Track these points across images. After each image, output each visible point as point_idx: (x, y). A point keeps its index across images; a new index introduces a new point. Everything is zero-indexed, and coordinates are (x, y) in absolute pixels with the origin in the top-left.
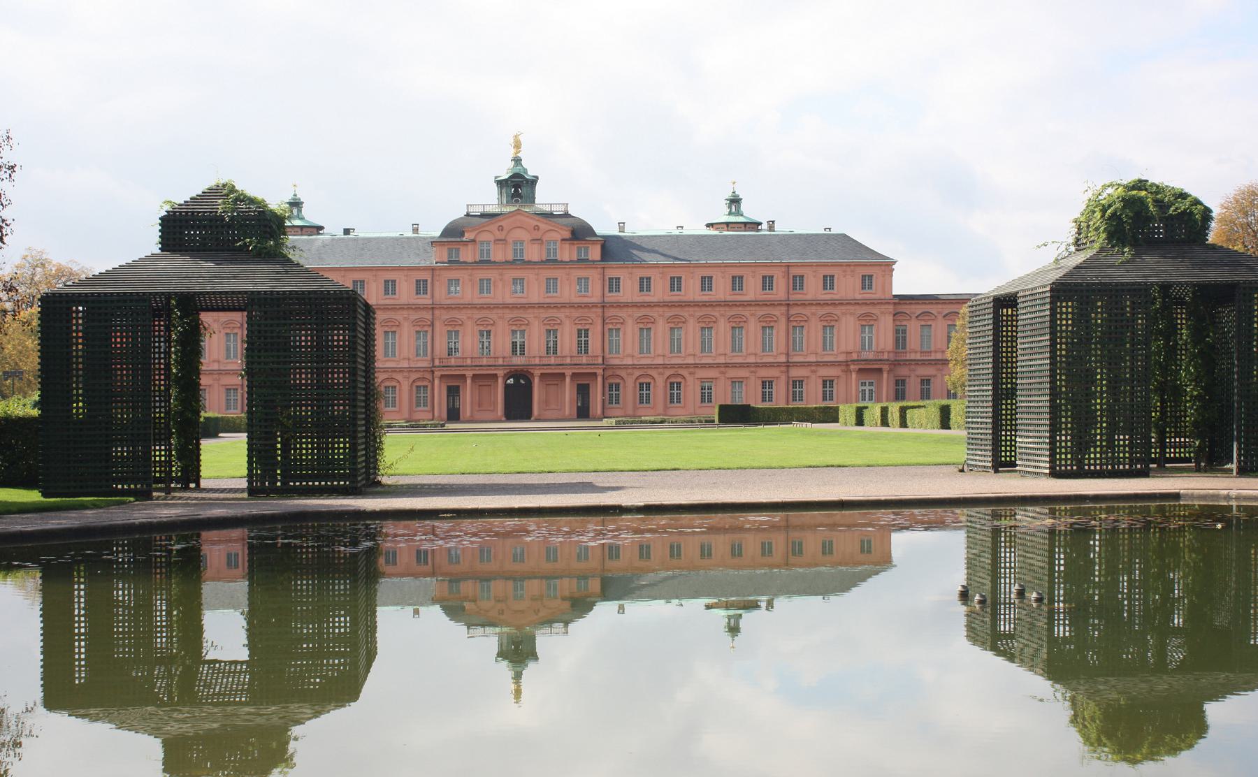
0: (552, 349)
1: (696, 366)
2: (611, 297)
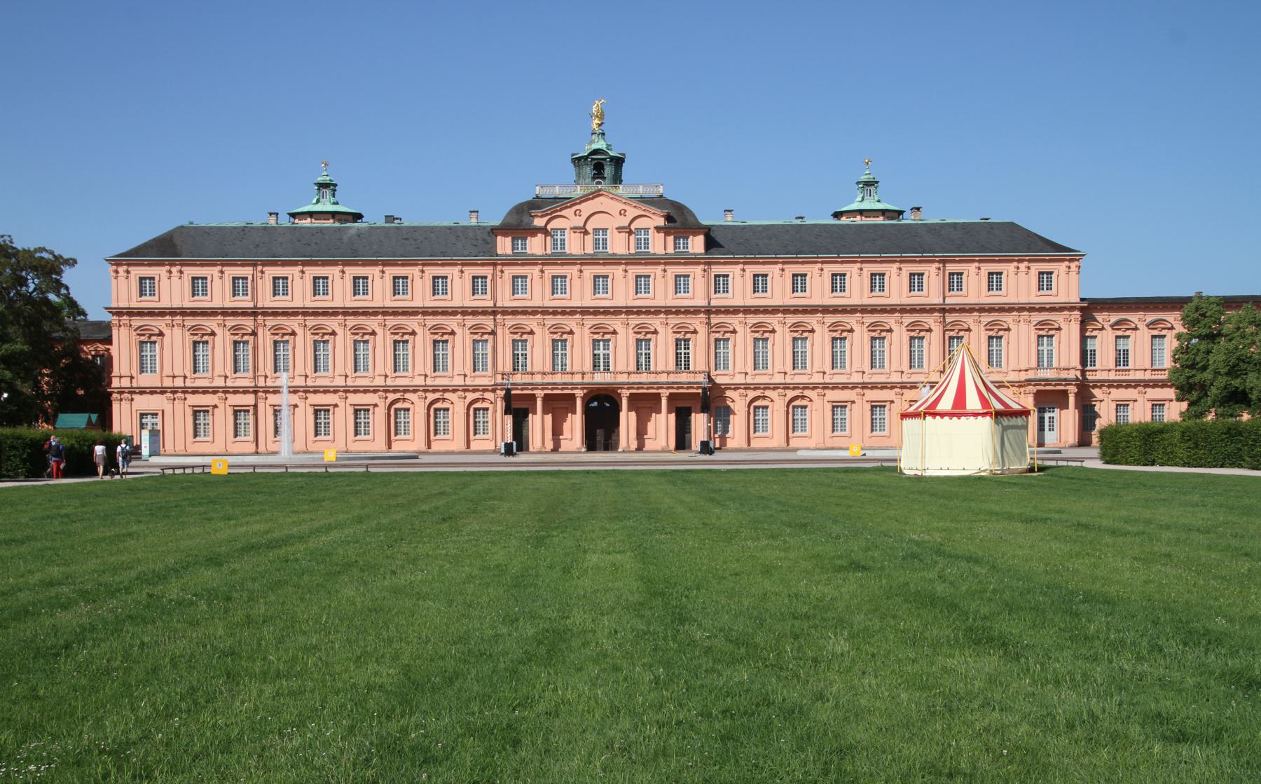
1: (826, 386)
2: (718, 301)
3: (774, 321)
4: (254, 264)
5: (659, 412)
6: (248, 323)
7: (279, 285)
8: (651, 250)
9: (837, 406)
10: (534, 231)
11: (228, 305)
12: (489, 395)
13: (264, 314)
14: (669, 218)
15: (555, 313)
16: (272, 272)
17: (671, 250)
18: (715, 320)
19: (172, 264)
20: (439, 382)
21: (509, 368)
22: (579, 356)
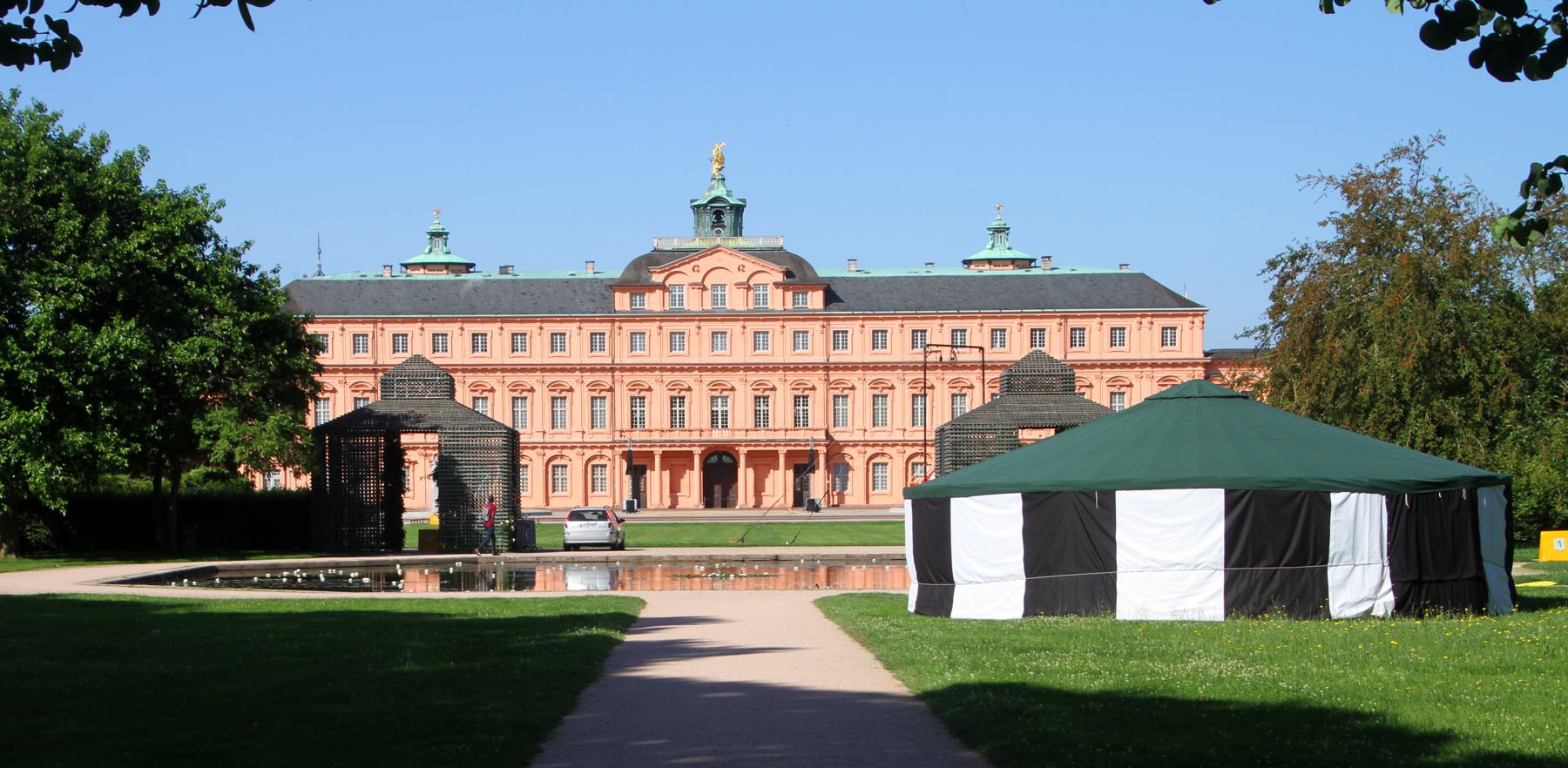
0: (761, 419)
2: (837, 357)
8: (769, 306)
10: (653, 288)
14: (788, 274)
17: (789, 306)
18: (834, 376)
20: (558, 438)
21: (627, 426)
22: (697, 412)
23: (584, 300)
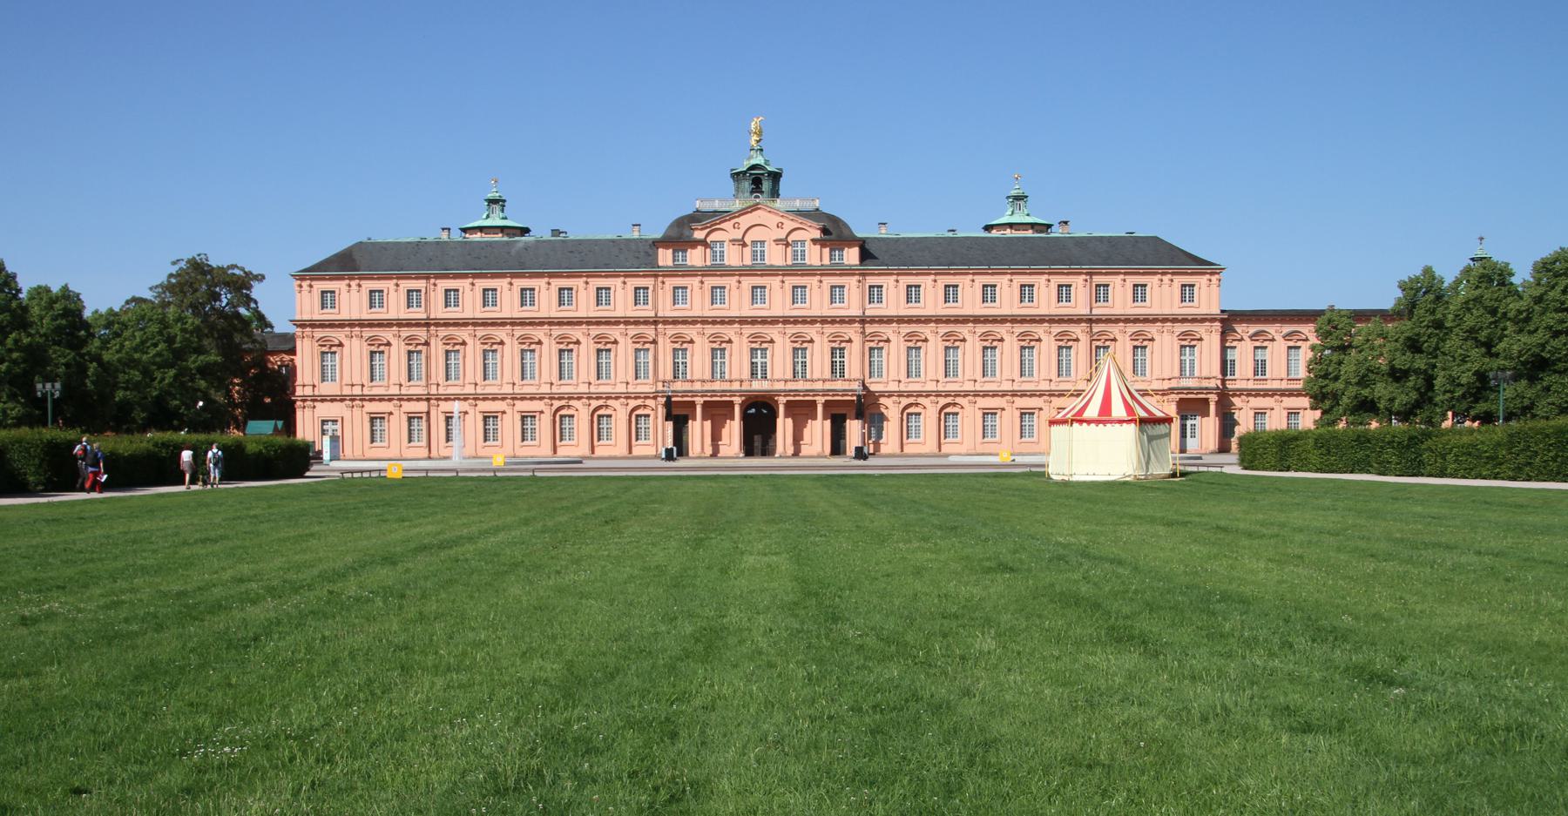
0: (798, 371)
1: (976, 394)
2: (873, 310)
3: (926, 330)
4: (427, 278)
5: (815, 418)
6: (421, 333)
7: (451, 297)
8: (807, 261)
9: (988, 413)
10: (695, 244)
11: (402, 316)
12: (650, 402)
13: (437, 325)
14: (825, 231)
15: (714, 323)
16: (444, 284)
17: (826, 261)
18: (869, 329)
19: (351, 278)
20: (602, 389)
21: (669, 376)
22: (737, 365)
23: (631, 257)
